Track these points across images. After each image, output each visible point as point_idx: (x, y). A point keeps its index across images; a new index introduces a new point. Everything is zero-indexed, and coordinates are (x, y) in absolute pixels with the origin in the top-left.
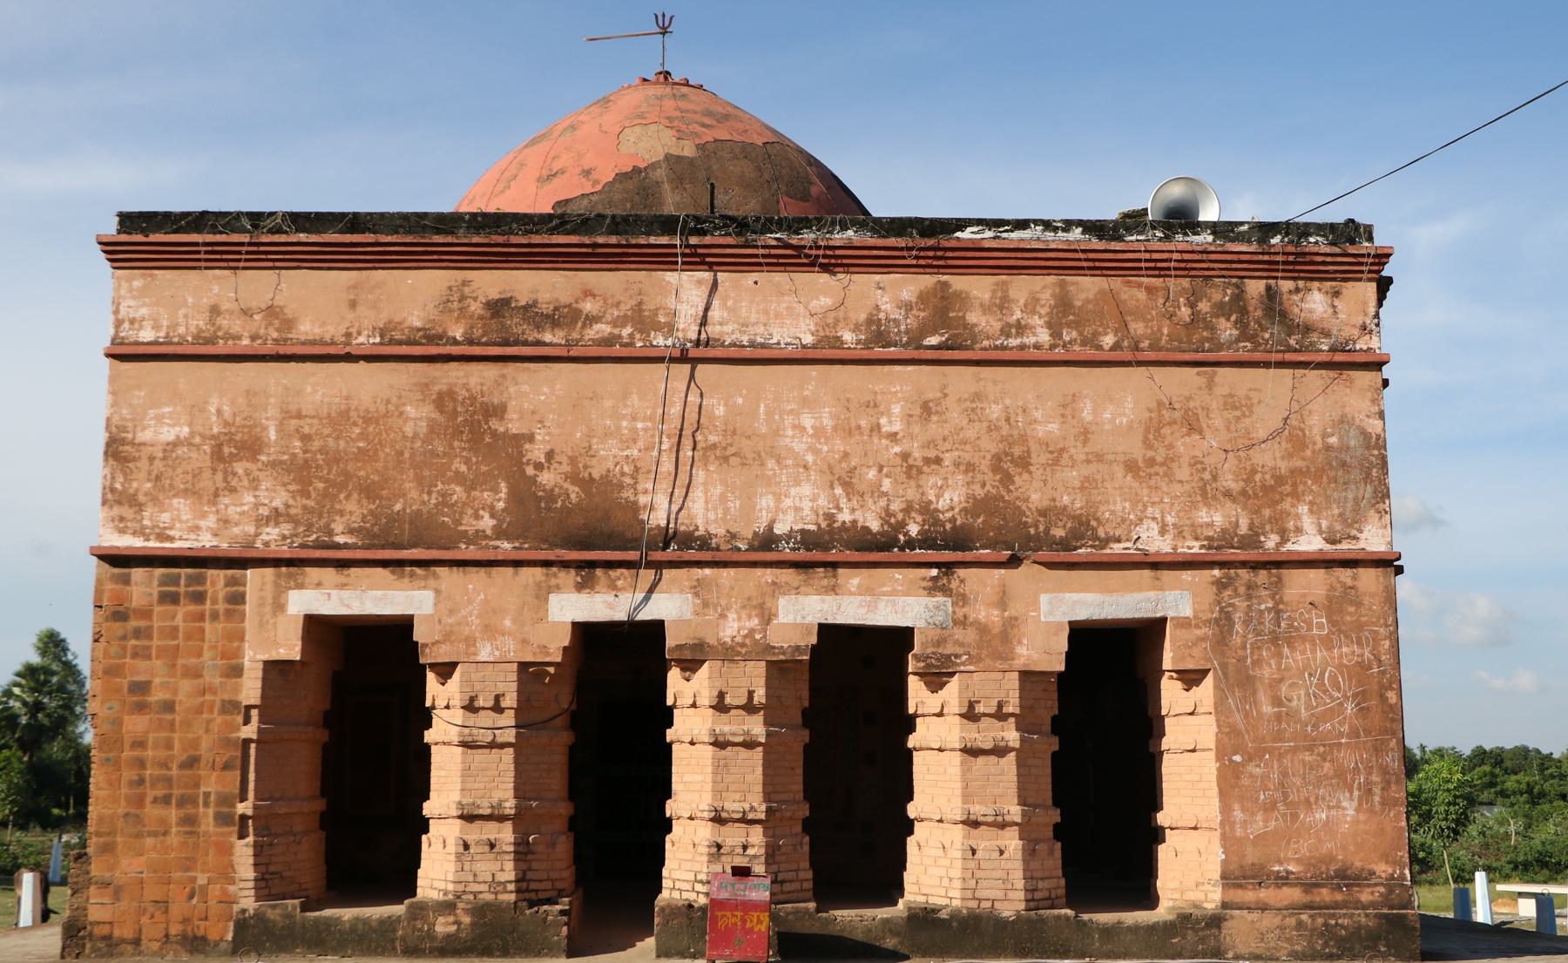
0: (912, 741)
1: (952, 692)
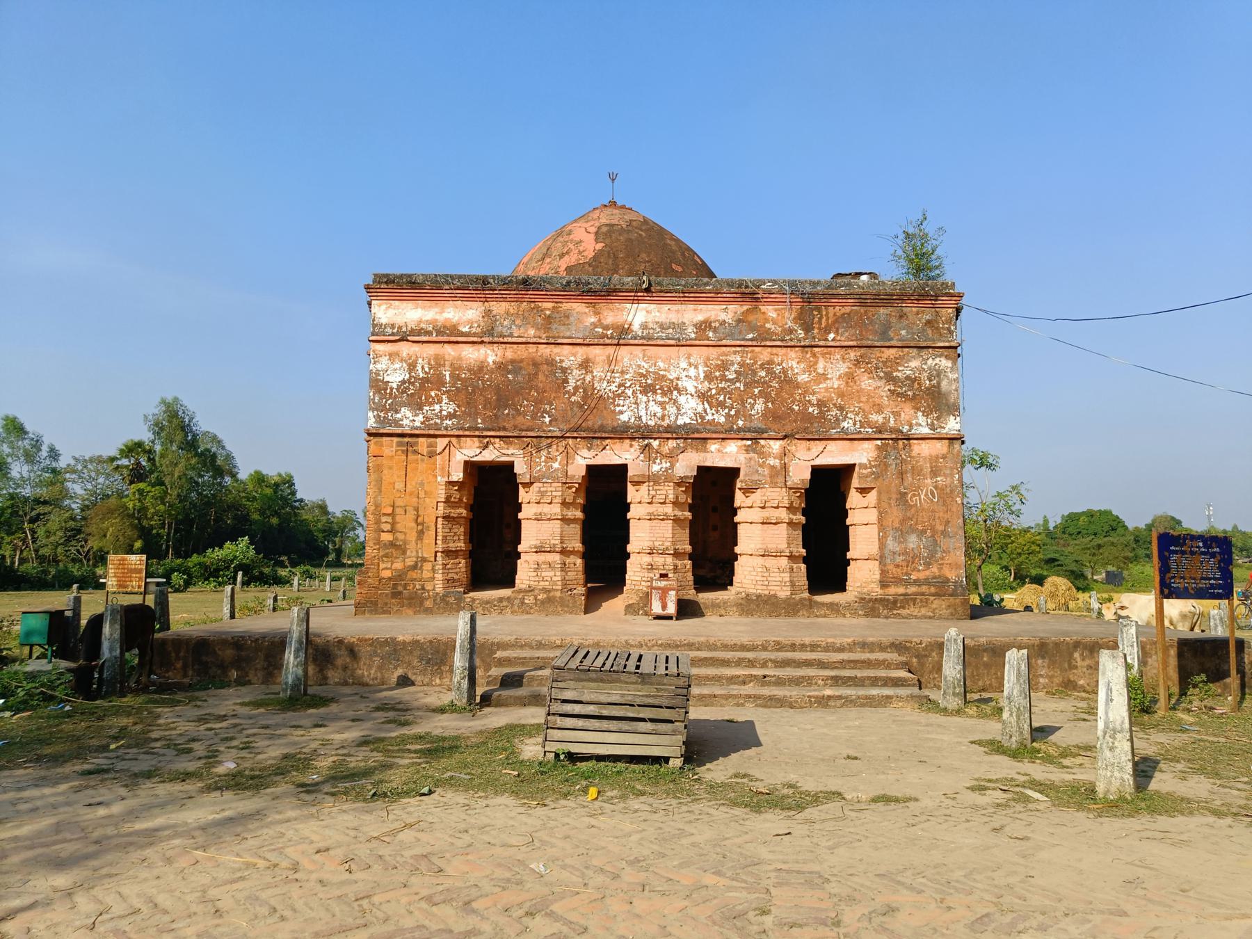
0: (736, 519)
1: (757, 497)
